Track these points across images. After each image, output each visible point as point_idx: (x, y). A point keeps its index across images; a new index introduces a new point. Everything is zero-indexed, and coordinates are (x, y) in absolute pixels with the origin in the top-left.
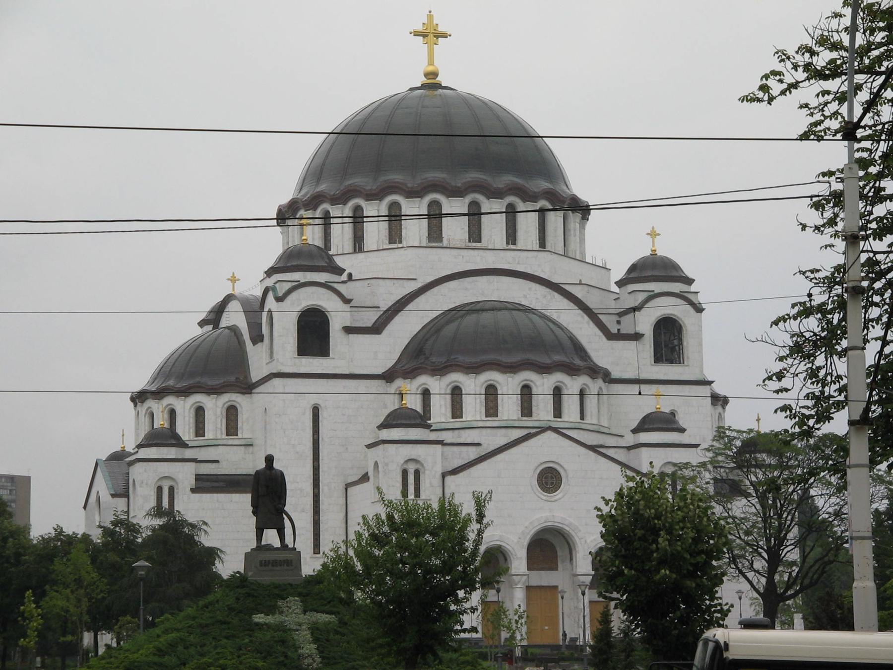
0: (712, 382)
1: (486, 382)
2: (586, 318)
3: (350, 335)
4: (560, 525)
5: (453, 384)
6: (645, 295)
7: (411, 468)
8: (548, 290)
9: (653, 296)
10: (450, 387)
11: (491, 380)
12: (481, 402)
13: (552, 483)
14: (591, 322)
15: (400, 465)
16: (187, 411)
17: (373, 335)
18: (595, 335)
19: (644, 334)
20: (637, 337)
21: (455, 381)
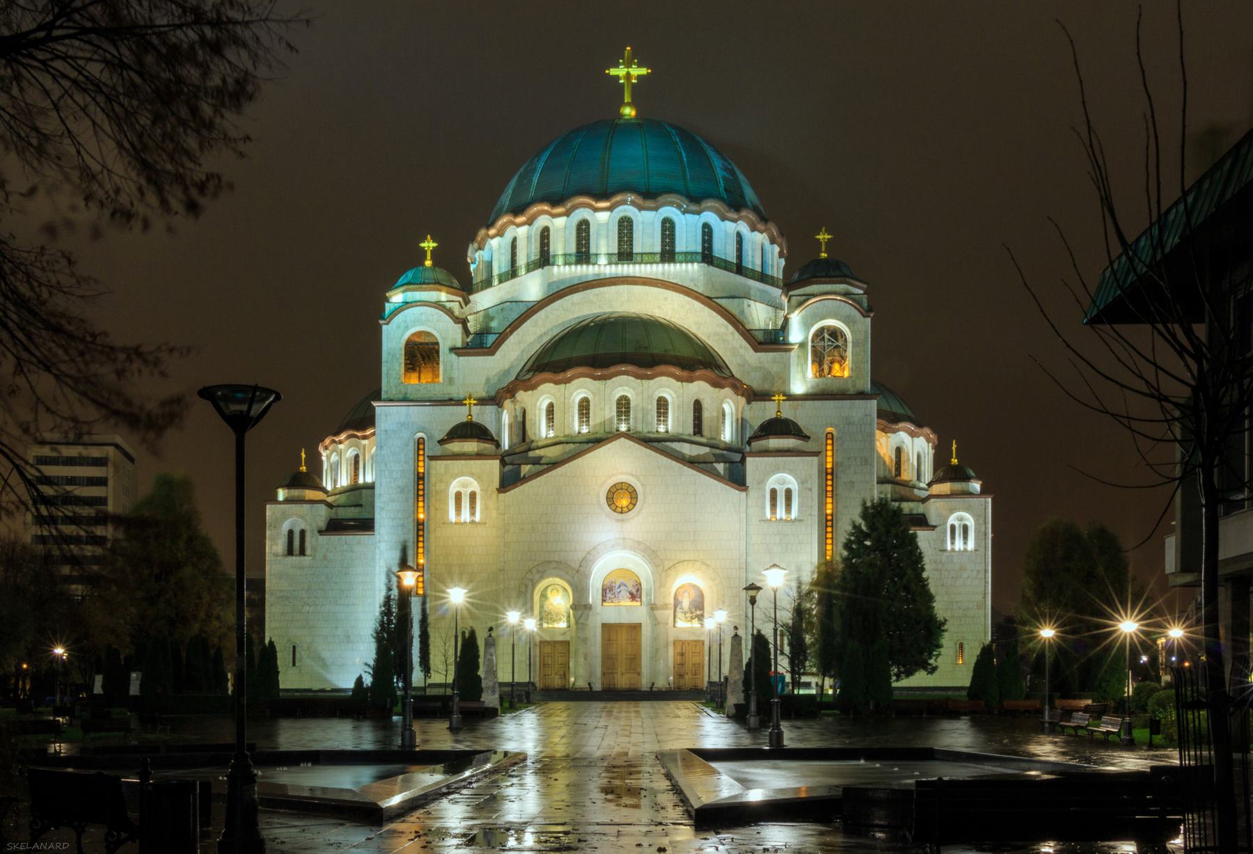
2: (731, 328)
8: (687, 298)
14: (737, 333)
18: (741, 347)
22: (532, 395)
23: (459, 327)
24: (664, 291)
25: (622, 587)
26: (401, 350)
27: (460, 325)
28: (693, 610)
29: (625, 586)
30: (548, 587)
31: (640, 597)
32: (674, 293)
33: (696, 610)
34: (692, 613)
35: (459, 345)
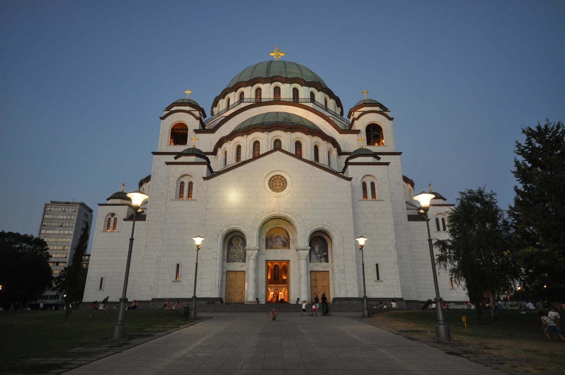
0: (402, 153)
1: (253, 139)
2: (328, 123)
3: (198, 134)
4: (285, 214)
5: (237, 144)
6: (361, 113)
7: (186, 181)
8: (306, 111)
9: (365, 113)
10: (236, 146)
11: (256, 138)
12: (250, 150)
13: (280, 186)
15: (177, 178)
16: (146, 189)
17: (210, 134)
18: (333, 132)
19: (360, 130)
20: (357, 132)
21: (238, 142)
22: (230, 143)
23: (198, 122)
24: (296, 107)
25: (278, 239)
26: (169, 130)
27: (199, 121)
28: (321, 253)
29: (280, 237)
30: (233, 237)
31: (289, 245)
32: (301, 109)
33: (323, 252)
34: (321, 254)
35: (198, 128)
